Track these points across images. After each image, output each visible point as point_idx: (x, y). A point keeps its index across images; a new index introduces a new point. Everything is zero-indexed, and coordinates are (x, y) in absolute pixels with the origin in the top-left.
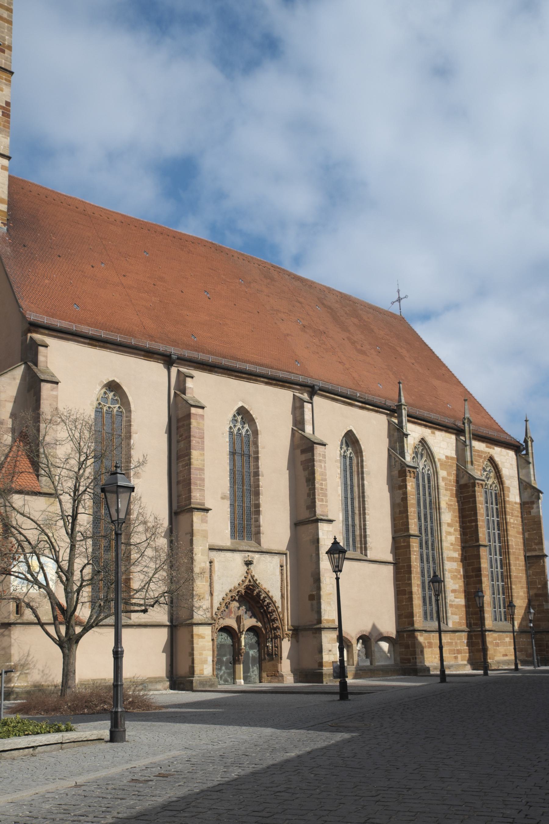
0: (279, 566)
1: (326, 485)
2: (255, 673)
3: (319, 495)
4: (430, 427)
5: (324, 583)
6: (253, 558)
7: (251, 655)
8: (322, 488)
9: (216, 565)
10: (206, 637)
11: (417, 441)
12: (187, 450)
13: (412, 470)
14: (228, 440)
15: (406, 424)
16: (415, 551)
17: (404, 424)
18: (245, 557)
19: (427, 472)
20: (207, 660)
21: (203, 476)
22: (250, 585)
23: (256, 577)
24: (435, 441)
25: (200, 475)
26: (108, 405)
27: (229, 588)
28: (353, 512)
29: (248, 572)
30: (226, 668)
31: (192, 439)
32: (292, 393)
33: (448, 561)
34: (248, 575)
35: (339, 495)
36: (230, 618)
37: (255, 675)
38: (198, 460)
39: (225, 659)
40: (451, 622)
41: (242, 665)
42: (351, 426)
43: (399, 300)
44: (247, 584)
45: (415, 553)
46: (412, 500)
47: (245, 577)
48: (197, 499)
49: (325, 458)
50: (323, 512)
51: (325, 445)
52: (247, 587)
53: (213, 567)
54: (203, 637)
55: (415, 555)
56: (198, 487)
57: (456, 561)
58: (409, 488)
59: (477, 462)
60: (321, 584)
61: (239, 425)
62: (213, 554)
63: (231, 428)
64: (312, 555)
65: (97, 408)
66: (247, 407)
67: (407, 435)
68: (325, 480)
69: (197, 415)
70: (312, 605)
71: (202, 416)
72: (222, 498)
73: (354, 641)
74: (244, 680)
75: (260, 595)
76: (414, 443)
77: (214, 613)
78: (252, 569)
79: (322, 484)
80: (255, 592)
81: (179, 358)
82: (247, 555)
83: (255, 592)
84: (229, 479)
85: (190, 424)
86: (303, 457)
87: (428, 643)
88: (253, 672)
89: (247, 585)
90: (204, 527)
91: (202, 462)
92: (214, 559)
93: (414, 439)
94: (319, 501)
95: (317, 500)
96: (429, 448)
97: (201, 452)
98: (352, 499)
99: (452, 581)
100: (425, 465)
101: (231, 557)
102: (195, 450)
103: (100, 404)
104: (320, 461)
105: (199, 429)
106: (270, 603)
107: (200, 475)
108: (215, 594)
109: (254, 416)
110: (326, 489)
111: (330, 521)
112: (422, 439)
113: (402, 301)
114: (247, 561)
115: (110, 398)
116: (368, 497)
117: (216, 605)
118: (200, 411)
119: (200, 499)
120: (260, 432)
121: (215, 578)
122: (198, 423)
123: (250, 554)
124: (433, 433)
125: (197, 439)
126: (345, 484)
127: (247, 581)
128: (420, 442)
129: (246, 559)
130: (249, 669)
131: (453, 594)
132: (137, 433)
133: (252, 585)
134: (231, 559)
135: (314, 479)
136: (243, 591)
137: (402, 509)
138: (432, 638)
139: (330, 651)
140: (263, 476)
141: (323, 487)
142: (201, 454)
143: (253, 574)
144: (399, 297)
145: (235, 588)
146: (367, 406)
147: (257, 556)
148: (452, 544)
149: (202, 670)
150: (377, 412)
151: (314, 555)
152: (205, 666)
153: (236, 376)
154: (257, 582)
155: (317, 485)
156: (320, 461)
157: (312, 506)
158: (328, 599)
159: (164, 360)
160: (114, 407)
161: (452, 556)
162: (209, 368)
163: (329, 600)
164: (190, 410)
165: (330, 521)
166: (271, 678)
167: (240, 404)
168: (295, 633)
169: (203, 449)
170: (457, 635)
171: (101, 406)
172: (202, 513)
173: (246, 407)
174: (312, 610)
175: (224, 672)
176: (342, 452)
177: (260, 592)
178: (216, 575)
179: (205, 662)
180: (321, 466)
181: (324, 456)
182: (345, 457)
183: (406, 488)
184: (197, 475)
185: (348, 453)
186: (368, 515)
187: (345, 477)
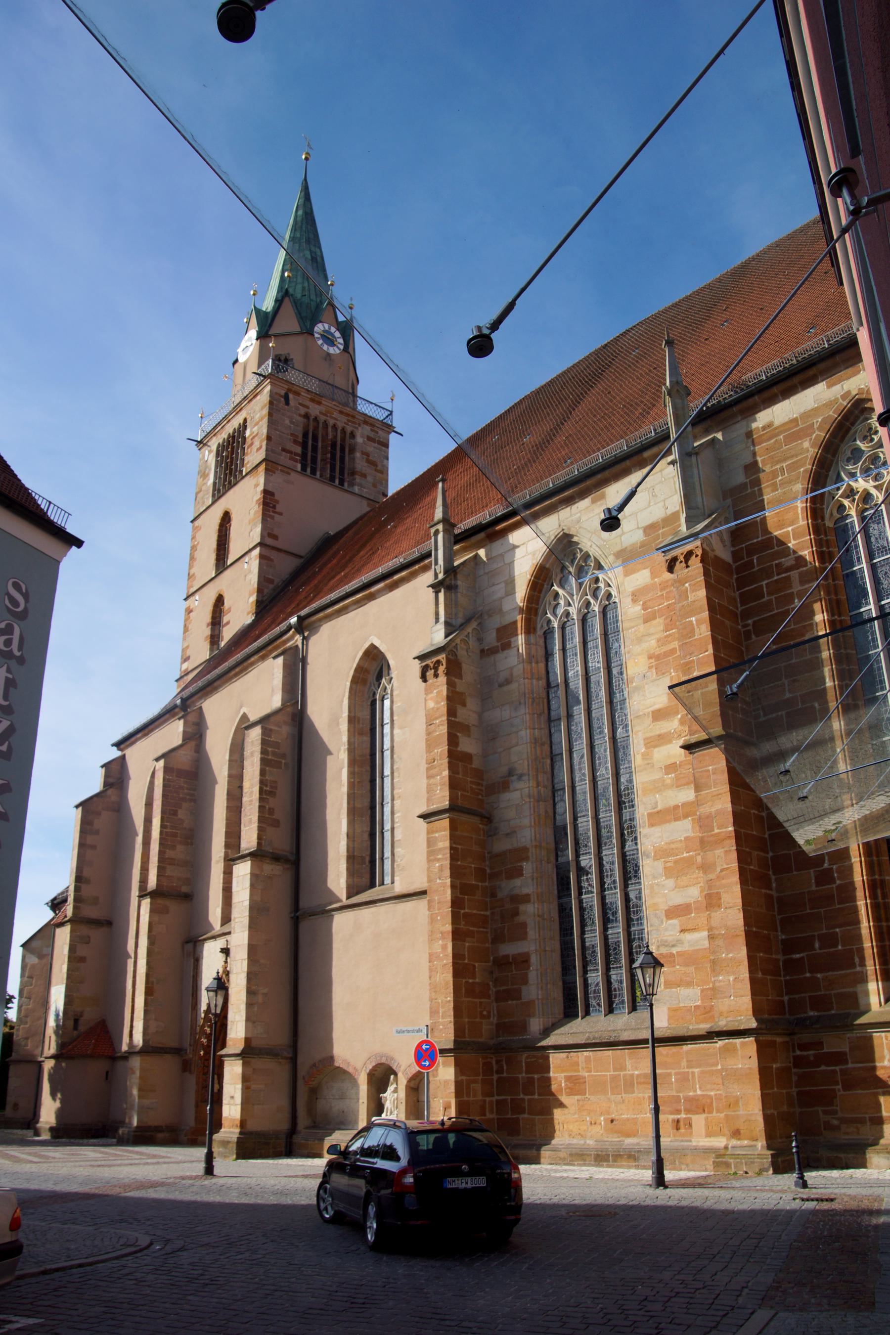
4: (582, 495)
33: (651, 825)
40: (665, 1009)
45: (440, 856)
50: (250, 842)
55: (438, 860)
57: (686, 816)
59: (785, 460)
87: (568, 1079)
99: (670, 883)
131: (675, 922)
138: (582, 1064)
146: (396, 577)
148: (671, 768)
161: (672, 803)
170: (688, 1052)
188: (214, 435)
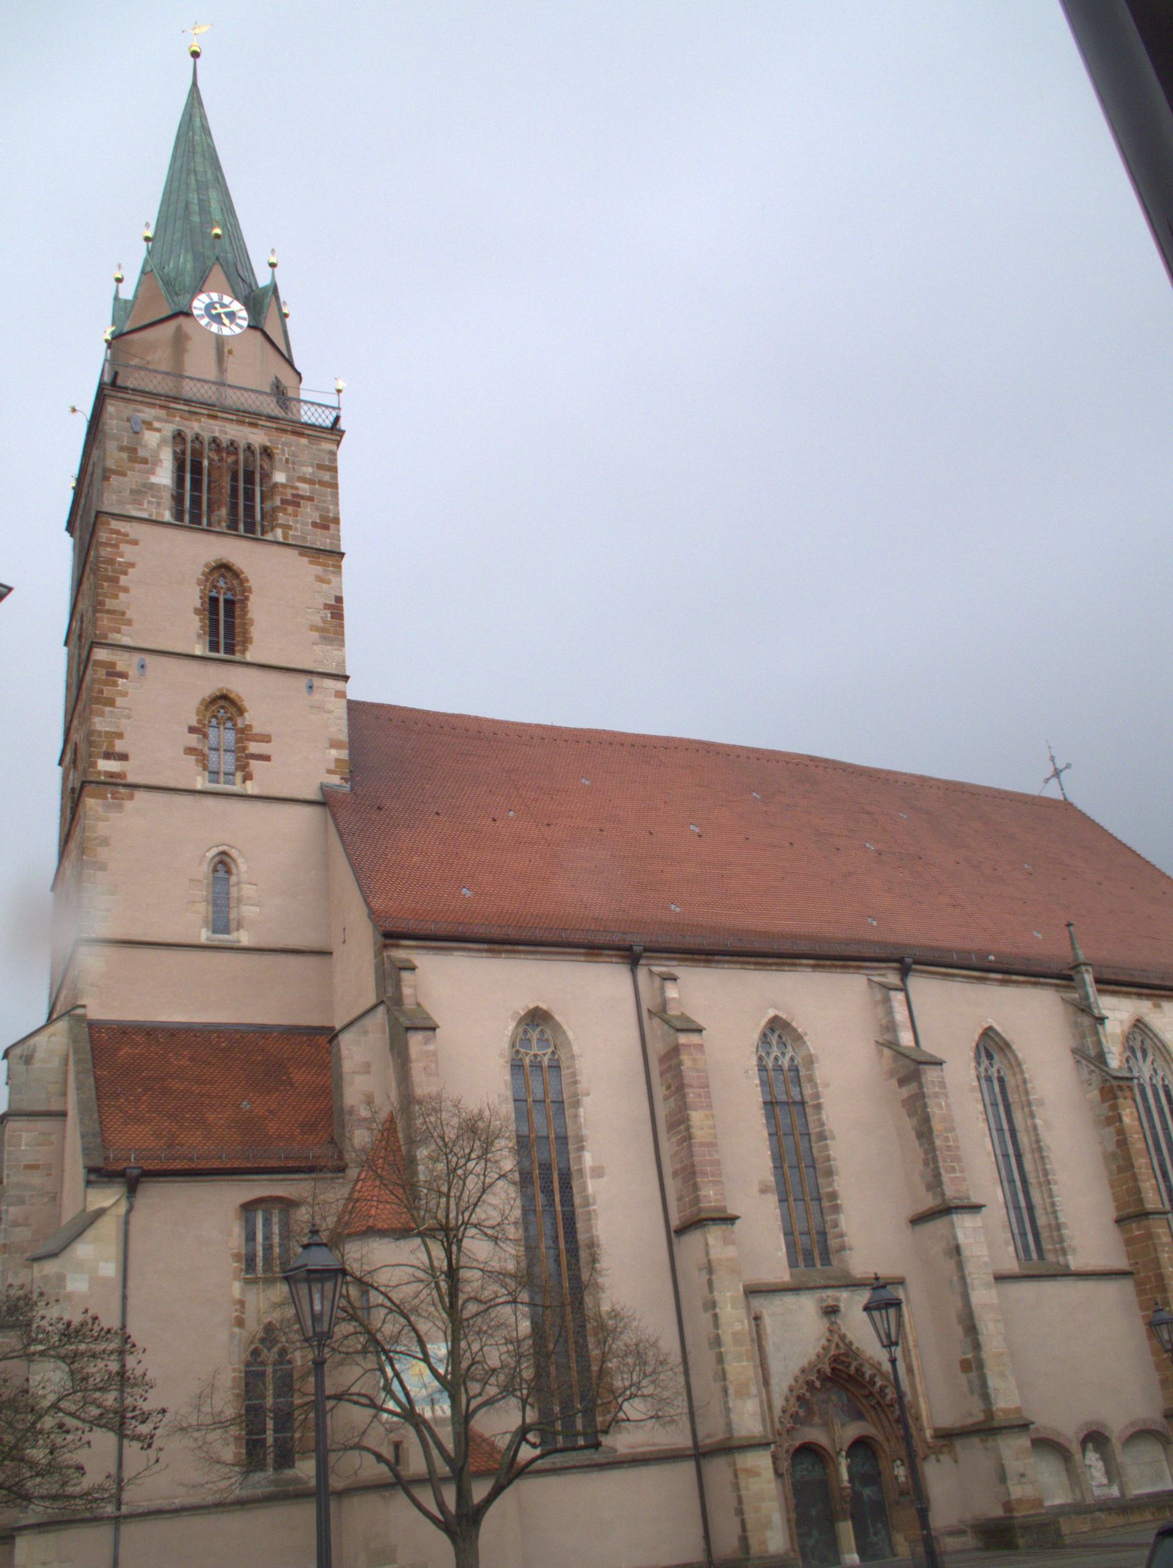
1: (956, 1139)
3: (944, 1161)
4: (1149, 997)
5: (985, 1333)
6: (837, 1299)
8: (948, 1146)
11: (1126, 1027)
12: (680, 1112)
13: (1123, 1083)
14: (757, 1081)
15: (1096, 1000)
16: (1166, 1244)
17: (1092, 999)
18: (822, 1300)
19: (1161, 1082)
21: (716, 1157)
22: (840, 1354)
23: (850, 1336)
24: (1165, 1020)
25: (710, 1155)
26: (532, 1053)
28: (1024, 1181)
31: (687, 1090)
32: (865, 977)
34: (832, 1336)
35: (989, 1154)
38: (702, 1129)
39: (814, 1512)
41: (849, 1524)
42: (989, 1020)
43: (1057, 773)
44: (832, 1353)
46: (1137, 1143)
47: (829, 1340)
48: (710, 1202)
49: (945, 1088)
51: (940, 1063)
52: (836, 1359)
53: (761, 1327)
54: (757, 1474)
56: (710, 1178)
58: (1126, 1120)
60: (979, 1337)
61: (775, 1051)
62: (758, 1303)
63: (760, 1058)
64: (951, 1281)
65: (513, 1060)
66: (784, 1017)
67: (1101, 1020)
68: (952, 1129)
69: (690, 1046)
70: (970, 1382)
71: (700, 1047)
72: (763, 1191)
73: (1075, 1447)
74: (859, 1553)
75: (863, 1374)
76: (1123, 1031)
77: (776, 1420)
78: (839, 1321)
79: (947, 1139)
81: (646, 950)
82: (824, 1295)
84: (769, 1153)
85: (680, 1064)
86: (905, 1092)
88: (876, 1534)
89: (834, 1355)
90: (731, 1251)
91: (712, 1131)
92: (761, 1312)
93: (1122, 1022)
94: (947, 1172)
95: (942, 1171)
96: (1155, 1035)
97: (707, 1112)
98: (1019, 1157)
100: (1155, 1071)
102: (696, 1110)
103: (517, 1052)
104: (936, 1095)
105: (698, 1071)
106: (886, 1387)
107: (710, 1155)
108: (774, 1381)
109: (800, 1030)
110: (958, 1148)
111: (976, 1208)
112: (1138, 1020)
113: (1062, 775)
114: (826, 1307)
115: (535, 1037)
116: (1049, 1148)
117: (778, 1403)
118: (694, 1038)
119: (716, 1201)
120: (817, 1057)
121: (769, 1348)
122: (694, 1060)
123: (830, 1292)
124: (1158, 1006)
125: (697, 1090)
126: (1000, 1130)
127: (833, 1346)
128: (1135, 1026)
129: (824, 1304)
132: (588, 1095)
133: (843, 1354)
135: (930, 1130)
136: (828, 1370)
137: (1122, 1163)
139: (1022, 1475)
140: (833, 1138)
141: (951, 1143)
142: (707, 1117)
144: (1056, 769)
145: (812, 1365)
146: (1014, 978)
147: (844, 1295)
149: (763, 1543)
150: (1035, 984)
151: (955, 1279)
152: (769, 1534)
153: (756, 964)
154: (854, 1348)
155: (938, 1142)
156: (936, 1095)
157: (935, 1182)
159: (623, 957)
160: (545, 1055)
162: (704, 957)
164: (676, 1039)
165: (976, 1208)
167: (771, 1013)
169: (710, 1106)
171: (520, 1056)
172: (724, 1227)
173: (784, 1016)
174: (972, 1392)
176: (982, 1069)
177: (861, 1365)
179: (767, 1524)
180: (940, 1105)
181: (943, 1084)
182: (989, 1079)
183: (1120, 1120)
184: (704, 1155)
185: (994, 1070)
186: (1056, 1183)
187: (997, 1115)
188: (161, 407)
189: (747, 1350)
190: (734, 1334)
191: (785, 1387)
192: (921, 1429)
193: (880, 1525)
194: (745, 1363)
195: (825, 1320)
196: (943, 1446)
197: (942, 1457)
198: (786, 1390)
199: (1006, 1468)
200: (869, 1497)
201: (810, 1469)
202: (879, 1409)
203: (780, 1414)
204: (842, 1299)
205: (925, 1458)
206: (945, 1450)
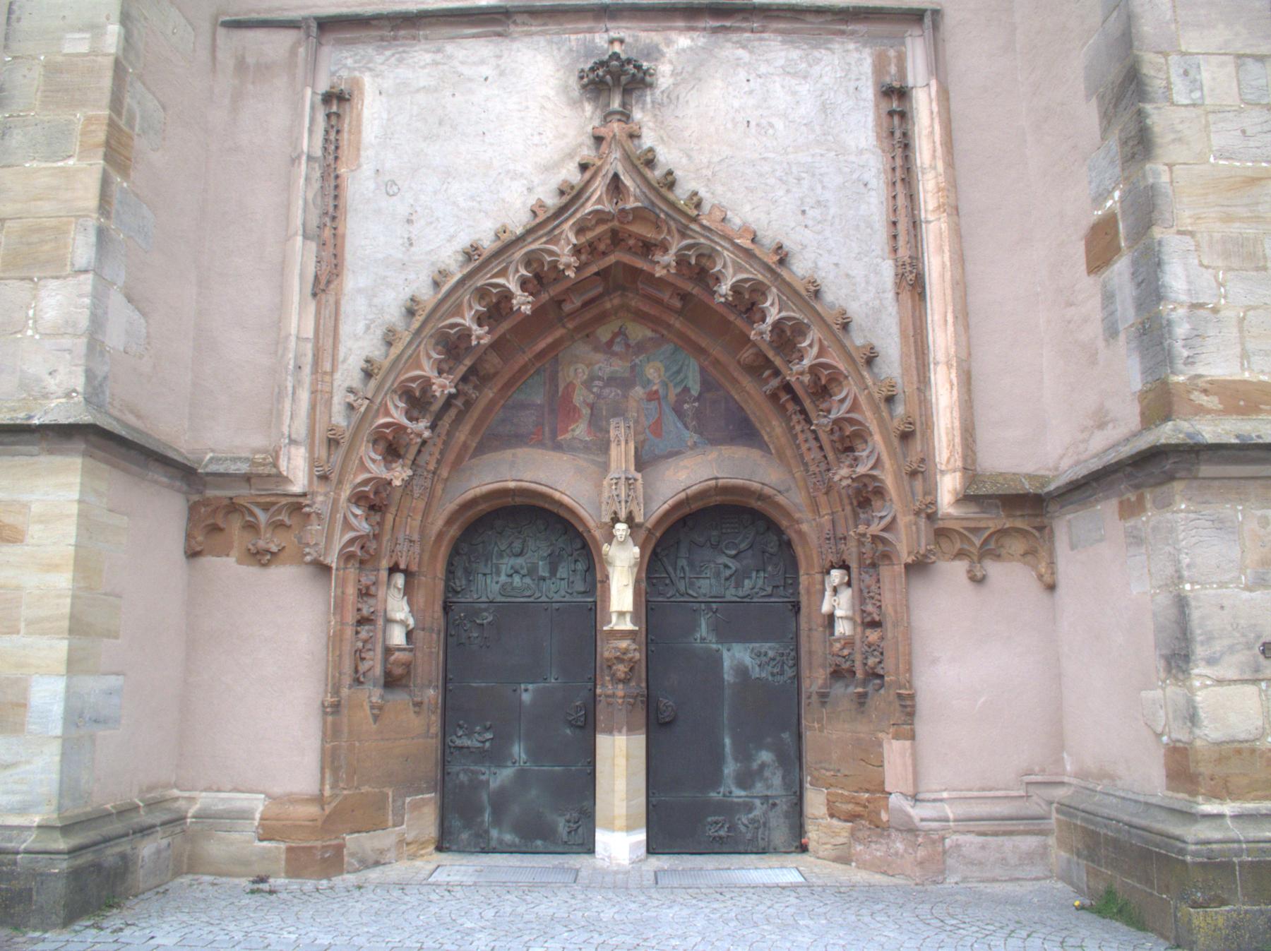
0: (869, 92)
2: (759, 788)
6: (653, 52)
7: (728, 676)
9: (366, 113)
10: (35, 532)
18: (589, 51)
20: (23, 705)
23: (667, 156)
27: (464, 241)
29: (603, 131)
30: (536, 754)
36: (558, 447)
37: (766, 798)
70: (1108, 298)
80: (667, 259)
82: (600, 39)
83: (667, 259)
88: (744, 780)
89: (600, 217)
92: (357, 83)
101: (483, 62)
106: (800, 330)
108: (354, 281)
127: (599, 187)
130: (719, 760)
133: (638, 215)
134: (486, 70)
143: (648, 140)
154: (681, 194)
158: (1228, 219)
163: (1235, 228)
166: (853, 834)
168: (1019, 524)
175: (522, 776)
178: (367, 169)
189: (89, 120)
190: (52, 69)
191: (391, 305)
192: (920, 472)
193: (766, 756)
194: (71, 162)
195: (588, 108)
196: (1002, 533)
197: (993, 569)
198: (393, 313)
199: (1195, 615)
200: (742, 671)
201: (543, 571)
202: (791, 407)
203: (355, 379)
204: (669, 52)
205: (918, 567)
206: (1016, 546)
